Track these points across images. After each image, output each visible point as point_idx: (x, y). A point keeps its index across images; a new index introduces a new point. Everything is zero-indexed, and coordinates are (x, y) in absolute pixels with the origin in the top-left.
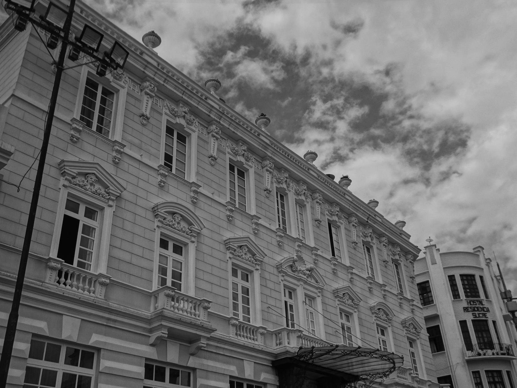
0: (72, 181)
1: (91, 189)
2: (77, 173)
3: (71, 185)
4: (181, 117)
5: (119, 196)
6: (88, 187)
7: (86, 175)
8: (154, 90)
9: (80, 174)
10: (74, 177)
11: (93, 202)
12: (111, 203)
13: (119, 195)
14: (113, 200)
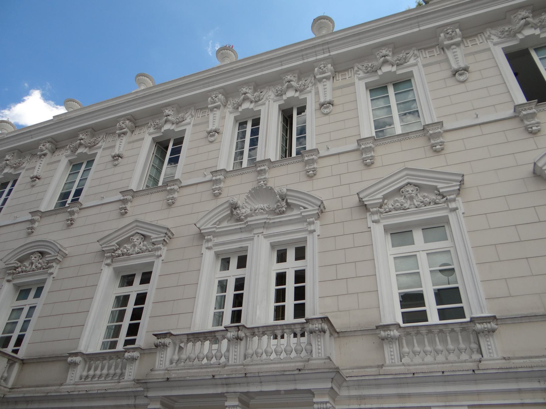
0: (382, 210)
1: (414, 204)
2: (382, 197)
3: (383, 214)
4: (522, 29)
5: (459, 190)
6: (406, 205)
8: (456, 34)
9: (385, 197)
13: (458, 187)
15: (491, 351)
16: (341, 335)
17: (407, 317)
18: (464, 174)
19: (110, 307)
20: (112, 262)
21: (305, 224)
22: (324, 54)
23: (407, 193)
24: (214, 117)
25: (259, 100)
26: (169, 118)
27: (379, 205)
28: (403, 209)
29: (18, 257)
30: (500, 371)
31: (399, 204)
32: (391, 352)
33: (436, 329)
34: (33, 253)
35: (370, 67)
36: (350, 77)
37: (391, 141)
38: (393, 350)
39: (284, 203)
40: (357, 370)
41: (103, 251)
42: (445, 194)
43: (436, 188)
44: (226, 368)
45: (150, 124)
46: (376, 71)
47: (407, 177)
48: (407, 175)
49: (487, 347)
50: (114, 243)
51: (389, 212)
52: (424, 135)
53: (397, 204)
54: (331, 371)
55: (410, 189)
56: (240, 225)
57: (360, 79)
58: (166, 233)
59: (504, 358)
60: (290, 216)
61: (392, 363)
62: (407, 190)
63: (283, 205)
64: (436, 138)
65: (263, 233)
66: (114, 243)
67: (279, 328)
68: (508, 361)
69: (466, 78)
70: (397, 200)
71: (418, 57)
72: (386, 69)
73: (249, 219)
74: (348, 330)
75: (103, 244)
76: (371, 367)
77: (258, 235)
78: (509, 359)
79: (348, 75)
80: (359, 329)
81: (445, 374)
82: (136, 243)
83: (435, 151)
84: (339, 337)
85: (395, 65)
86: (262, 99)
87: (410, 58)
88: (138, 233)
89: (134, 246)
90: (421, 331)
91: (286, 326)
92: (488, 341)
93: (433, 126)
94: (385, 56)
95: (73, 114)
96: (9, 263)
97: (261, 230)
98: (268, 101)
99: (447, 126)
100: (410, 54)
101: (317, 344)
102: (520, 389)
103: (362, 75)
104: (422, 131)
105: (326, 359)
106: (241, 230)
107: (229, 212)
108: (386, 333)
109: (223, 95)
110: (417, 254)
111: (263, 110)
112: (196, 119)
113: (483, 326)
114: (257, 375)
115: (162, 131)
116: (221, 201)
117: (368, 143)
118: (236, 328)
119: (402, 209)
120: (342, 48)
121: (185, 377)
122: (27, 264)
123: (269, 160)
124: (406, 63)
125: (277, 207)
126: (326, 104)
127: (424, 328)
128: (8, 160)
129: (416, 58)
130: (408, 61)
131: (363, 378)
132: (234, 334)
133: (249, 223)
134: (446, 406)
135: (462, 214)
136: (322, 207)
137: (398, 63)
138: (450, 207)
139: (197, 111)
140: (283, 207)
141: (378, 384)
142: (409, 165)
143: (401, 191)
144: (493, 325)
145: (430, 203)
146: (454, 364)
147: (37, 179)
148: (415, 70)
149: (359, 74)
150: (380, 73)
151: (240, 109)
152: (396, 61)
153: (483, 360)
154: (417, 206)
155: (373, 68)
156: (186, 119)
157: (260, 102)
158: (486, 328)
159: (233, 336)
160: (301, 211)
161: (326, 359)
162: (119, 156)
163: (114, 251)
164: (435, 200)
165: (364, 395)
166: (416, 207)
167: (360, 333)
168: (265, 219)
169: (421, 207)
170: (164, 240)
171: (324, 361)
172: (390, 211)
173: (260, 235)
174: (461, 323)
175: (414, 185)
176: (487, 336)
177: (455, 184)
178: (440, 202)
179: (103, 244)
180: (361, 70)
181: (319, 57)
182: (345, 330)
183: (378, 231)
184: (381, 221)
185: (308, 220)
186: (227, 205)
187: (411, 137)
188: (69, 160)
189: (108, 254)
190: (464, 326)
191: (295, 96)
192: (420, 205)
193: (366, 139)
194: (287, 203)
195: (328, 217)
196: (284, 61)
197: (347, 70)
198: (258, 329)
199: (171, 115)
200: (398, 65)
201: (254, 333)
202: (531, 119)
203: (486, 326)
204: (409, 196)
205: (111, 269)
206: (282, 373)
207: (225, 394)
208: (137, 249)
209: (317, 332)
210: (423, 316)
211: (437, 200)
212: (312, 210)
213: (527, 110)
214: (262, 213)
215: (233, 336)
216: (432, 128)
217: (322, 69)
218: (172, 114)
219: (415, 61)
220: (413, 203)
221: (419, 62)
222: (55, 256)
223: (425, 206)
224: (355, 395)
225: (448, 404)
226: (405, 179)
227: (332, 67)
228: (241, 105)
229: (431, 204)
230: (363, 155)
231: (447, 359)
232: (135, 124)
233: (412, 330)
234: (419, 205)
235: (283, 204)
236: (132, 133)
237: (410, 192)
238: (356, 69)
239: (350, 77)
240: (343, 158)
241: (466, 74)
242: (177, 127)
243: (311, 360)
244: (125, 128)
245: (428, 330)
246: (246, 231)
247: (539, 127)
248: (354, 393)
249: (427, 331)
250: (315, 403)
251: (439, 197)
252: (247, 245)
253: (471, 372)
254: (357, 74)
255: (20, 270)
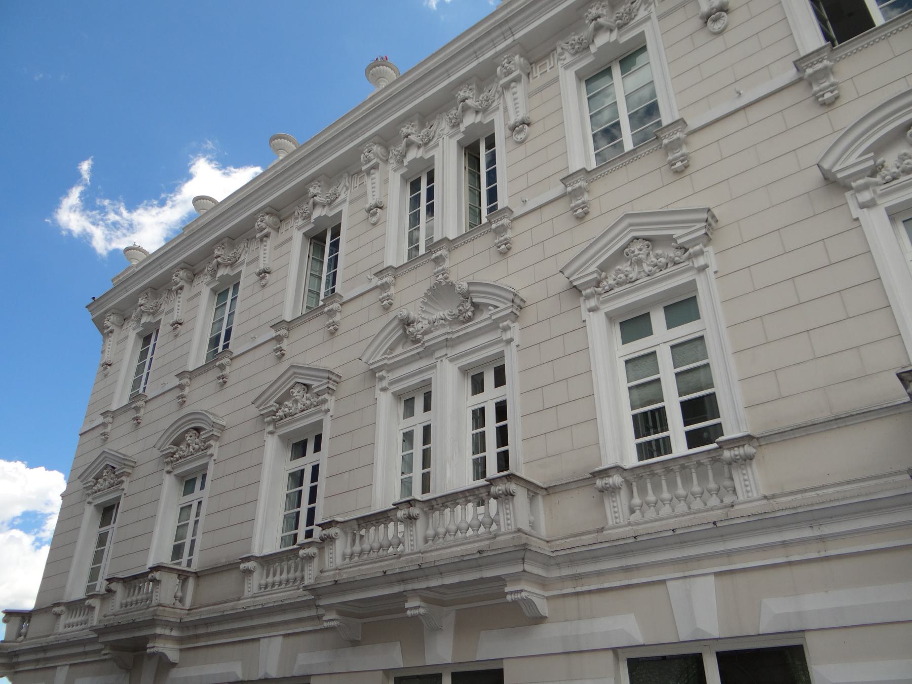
7: (621, 254)
9: (603, 268)
10: (598, 283)
11: (678, 283)
12: (700, 261)
14: (701, 253)
15: (748, 488)
16: (551, 491)
17: (645, 451)
18: (711, 207)
19: (283, 489)
20: (276, 428)
21: (499, 331)
22: (506, 40)
23: (632, 255)
24: (373, 184)
25: (430, 140)
26: (317, 199)
27: (594, 283)
28: (630, 282)
29: (172, 440)
30: (752, 519)
31: (622, 275)
32: (614, 507)
33: (676, 465)
34: (187, 431)
35: (578, 43)
36: (553, 67)
37: (612, 169)
38: (617, 504)
39: (468, 305)
40: (572, 539)
41: (261, 415)
42: (686, 246)
43: (670, 239)
44: (402, 559)
45: (296, 213)
46: (588, 47)
47: (629, 229)
48: (631, 225)
49: (743, 483)
50: (272, 403)
51: (610, 290)
52: (659, 147)
53: (619, 276)
54: (517, 549)
55: (636, 247)
56: (417, 348)
57: (567, 67)
58: (328, 378)
59: (765, 497)
60: (477, 323)
61: (617, 523)
62: (633, 249)
63: (468, 308)
64: (676, 149)
65: (446, 355)
66: (272, 403)
67: (461, 496)
68: (772, 501)
69: (724, 25)
70: (619, 270)
71: (650, 4)
72: (602, 39)
73: (426, 338)
74: (558, 484)
75: (261, 405)
76: (589, 533)
77: (441, 359)
78: (774, 497)
79: (550, 64)
80: (572, 480)
81: (678, 532)
82: (296, 397)
83: (677, 172)
84: (549, 494)
85: (614, 29)
86: (433, 137)
87: (638, 10)
88: (299, 383)
89: (296, 401)
90: (656, 470)
91: (469, 492)
92: (744, 474)
93: (669, 130)
94: (595, 19)
95: (205, 219)
96: (164, 449)
97: (443, 352)
98: (441, 139)
99: (693, 124)
100: (638, 2)
101: (505, 513)
102: (784, 541)
103: (568, 58)
104: (656, 140)
105: (515, 532)
106: (419, 356)
107: (401, 332)
108: (604, 481)
109: (380, 144)
110: (656, 349)
111: (436, 153)
112: (352, 190)
113: (732, 452)
114: (433, 565)
115: (312, 221)
116: (391, 315)
117: (573, 183)
118: (406, 503)
119: (628, 282)
120: (531, 22)
121: (354, 577)
122: (183, 447)
123: (445, 240)
124: (633, 19)
125: (459, 313)
126: (518, 126)
127: (658, 467)
128: (142, 305)
129: (647, 7)
130: (635, 16)
131: (572, 551)
132: (405, 512)
133: (427, 344)
134: (685, 577)
135: (713, 274)
136: (517, 301)
137: (618, 24)
138: (696, 265)
139: (352, 177)
140: (467, 311)
141: (593, 556)
142: (638, 208)
143: (625, 254)
144: (748, 449)
145: (667, 264)
146: (696, 516)
147: (179, 326)
148: (646, 28)
149: (565, 59)
150: (593, 49)
151: (406, 163)
152: (616, 21)
153: (736, 505)
154: (649, 273)
155: (582, 44)
156: (339, 195)
157: (432, 143)
158: (736, 456)
159: (404, 515)
160: (490, 313)
161: (515, 532)
162: (266, 272)
163: (274, 413)
164: (674, 259)
165: (580, 574)
166: (648, 275)
167: (574, 486)
168: (445, 334)
169: (655, 273)
170: (328, 387)
171: (511, 536)
172: (611, 289)
173: (444, 359)
174: (709, 451)
175: (644, 239)
176: (743, 467)
177: (698, 226)
178: (681, 261)
179: (261, 405)
180: (567, 50)
181: (500, 47)
182: (554, 485)
183: (597, 324)
184: (602, 307)
185: (501, 325)
186: (396, 322)
187: (641, 155)
188: (212, 289)
189: (268, 419)
190: (714, 455)
191: (418, 156)
192: (653, 271)
193: (574, 176)
194: (474, 304)
195: (530, 315)
196: (451, 68)
197: (547, 56)
198: (436, 501)
199: (318, 193)
200: (620, 27)
201: (432, 506)
202: (824, 78)
203: (737, 453)
204: (635, 259)
205: (276, 437)
206: (462, 558)
207: (405, 593)
208: (300, 406)
209: (503, 496)
210: (664, 446)
211: (677, 259)
212: (504, 308)
213: (816, 64)
214: (443, 326)
215: (404, 515)
216: (667, 133)
217: (506, 68)
218: (320, 192)
219: (646, 13)
220: (642, 270)
221: (652, 12)
222: (210, 431)
223: (661, 270)
224: (568, 575)
225: (687, 574)
226: (629, 232)
227: (522, 59)
228: (405, 156)
229: (669, 265)
230: (668, 156)
231: (690, 508)
232: (279, 217)
233: (642, 471)
234: (650, 271)
235: (466, 307)
236: (278, 232)
237: (637, 252)
238: (559, 50)
239: (553, 67)
240: (547, 213)
241: (723, 17)
242: (331, 210)
243: (499, 535)
244: (266, 228)
245: (665, 468)
246: (426, 356)
247: (836, 92)
248: (566, 572)
249: (664, 470)
250: (507, 593)
251: (679, 253)
252: (429, 377)
253: (712, 526)
254: (562, 60)
255: (177, 456)
